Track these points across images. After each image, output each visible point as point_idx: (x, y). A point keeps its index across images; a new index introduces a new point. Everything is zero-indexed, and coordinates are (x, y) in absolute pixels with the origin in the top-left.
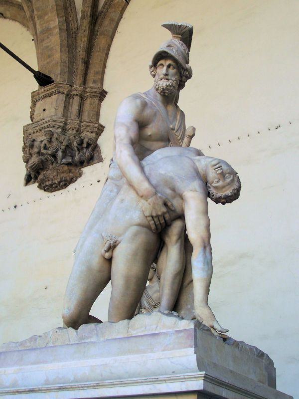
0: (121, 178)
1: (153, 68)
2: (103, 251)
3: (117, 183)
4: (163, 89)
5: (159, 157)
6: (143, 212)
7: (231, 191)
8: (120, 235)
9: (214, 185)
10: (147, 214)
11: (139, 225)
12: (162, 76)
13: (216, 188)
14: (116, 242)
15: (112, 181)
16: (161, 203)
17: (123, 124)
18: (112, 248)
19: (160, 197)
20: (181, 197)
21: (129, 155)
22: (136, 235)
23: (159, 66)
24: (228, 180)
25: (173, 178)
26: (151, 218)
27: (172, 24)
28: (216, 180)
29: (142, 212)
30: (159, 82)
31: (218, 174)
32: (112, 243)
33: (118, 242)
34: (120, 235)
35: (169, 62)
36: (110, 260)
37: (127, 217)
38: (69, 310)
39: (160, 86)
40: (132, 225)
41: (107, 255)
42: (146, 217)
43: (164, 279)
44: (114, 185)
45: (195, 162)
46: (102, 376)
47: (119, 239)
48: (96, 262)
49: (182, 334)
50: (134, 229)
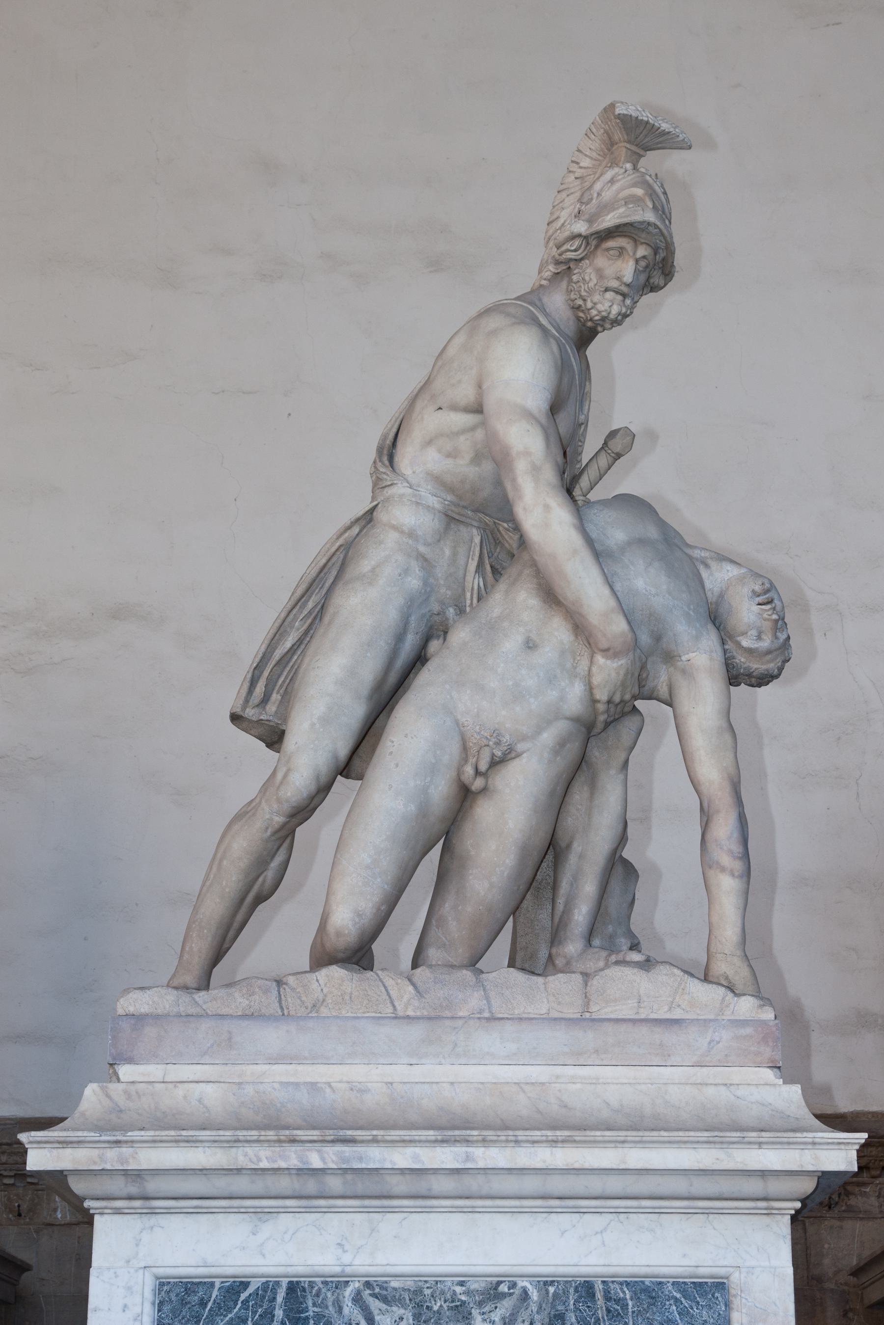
0: (439, 541)
1: (577, 243)
2: (469, 770)
3: (422, 549)
4: (604, 319)
8: (524, 738)
9: (745, 643)
10: (602, 695)
11: (576, 720)
12: (615, 284)
13: (750, 651)
14: (510, 753)
15: (410, 542)
17: (528, 415)
18: (496, 763)
20: (670, 658)
22: (561, 744)
24: (782, 637)
26: (606, 706)
27: (647, 122)
28: (754, 633)
29: (588, 687)
31: (765, 620)
32: (499, 753)
33: (513, 755)
37: (553, 695)
38: (359, 915)
39: (600, 307)
40: (557, 718)
41: (478, 783)
42: (594, 701)
43: (581, 857)
45: (697, 563)
47: (520, 747)
48: (441, 790)
49: (749, 1030)
50: (561, 727)
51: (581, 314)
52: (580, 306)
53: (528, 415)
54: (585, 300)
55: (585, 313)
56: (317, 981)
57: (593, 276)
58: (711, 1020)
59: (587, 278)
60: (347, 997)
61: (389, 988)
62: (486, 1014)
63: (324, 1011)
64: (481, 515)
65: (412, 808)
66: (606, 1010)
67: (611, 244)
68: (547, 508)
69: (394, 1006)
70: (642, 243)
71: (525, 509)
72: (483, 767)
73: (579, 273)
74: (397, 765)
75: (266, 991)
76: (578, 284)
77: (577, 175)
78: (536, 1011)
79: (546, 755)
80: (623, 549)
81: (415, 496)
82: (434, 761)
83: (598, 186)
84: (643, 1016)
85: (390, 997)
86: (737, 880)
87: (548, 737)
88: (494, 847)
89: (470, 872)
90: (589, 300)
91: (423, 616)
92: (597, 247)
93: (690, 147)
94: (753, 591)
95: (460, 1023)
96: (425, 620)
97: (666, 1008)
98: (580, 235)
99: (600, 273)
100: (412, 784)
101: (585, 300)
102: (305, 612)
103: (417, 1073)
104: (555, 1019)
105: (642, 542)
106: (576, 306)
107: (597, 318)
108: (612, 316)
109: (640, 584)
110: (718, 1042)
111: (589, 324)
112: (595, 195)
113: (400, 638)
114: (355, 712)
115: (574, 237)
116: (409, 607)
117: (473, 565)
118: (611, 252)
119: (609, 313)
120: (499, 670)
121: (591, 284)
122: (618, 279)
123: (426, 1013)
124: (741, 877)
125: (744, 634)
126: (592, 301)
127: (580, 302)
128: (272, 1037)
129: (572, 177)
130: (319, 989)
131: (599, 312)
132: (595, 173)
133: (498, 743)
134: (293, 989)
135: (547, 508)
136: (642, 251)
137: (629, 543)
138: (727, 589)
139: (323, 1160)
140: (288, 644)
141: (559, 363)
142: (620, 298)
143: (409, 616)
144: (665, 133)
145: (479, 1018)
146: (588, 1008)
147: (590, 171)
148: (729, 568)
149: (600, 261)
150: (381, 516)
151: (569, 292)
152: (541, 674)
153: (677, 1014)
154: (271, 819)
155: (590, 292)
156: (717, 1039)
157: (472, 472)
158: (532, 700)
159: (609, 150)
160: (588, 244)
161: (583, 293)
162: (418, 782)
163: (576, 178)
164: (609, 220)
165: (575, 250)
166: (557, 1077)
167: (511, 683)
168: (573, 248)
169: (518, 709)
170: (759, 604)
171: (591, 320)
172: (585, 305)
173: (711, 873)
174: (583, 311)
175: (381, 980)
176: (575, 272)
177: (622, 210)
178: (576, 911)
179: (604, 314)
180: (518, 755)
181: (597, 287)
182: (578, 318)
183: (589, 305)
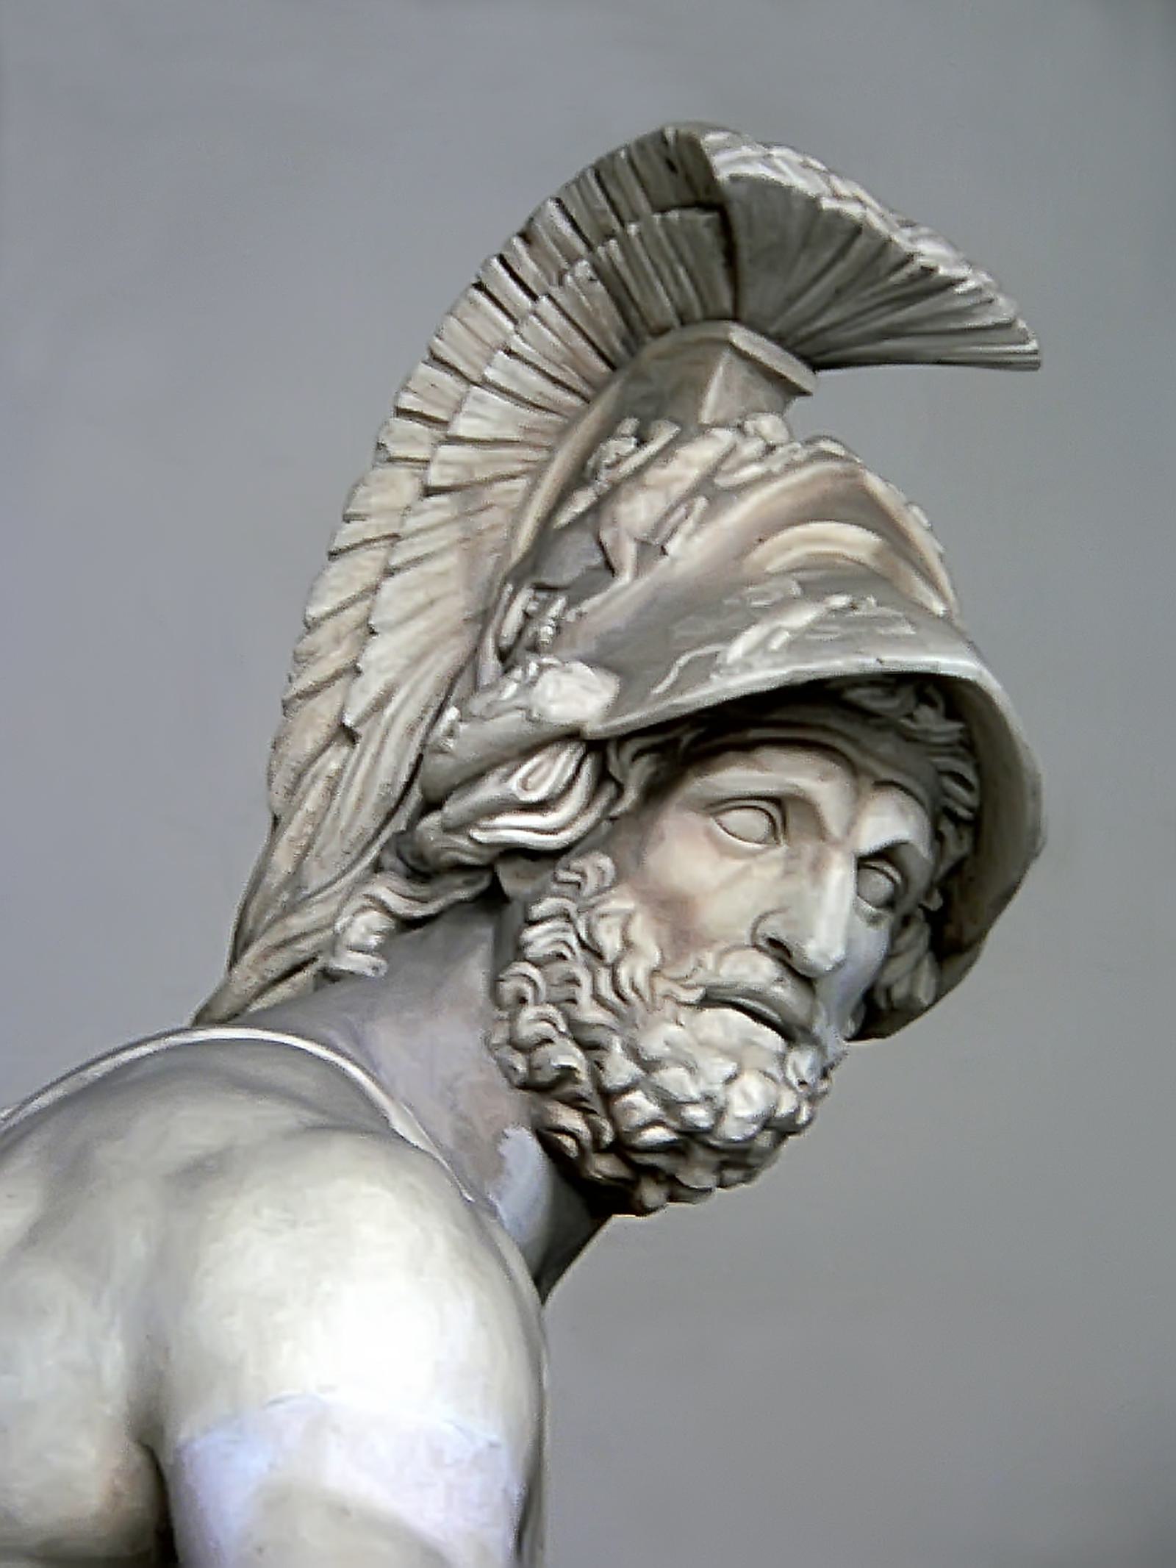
1: (553, 769)
23: (717, 807)
27: (857, 230)
35: (889, 822)
51: (571, 1119)
52: (567, 1074)
54: (589, 1047)
55: (586, 1112)
57: (642, 932)
59: (610, 942)
67: (735, 777)
70: (882, 784)
76: (559, 968)
90: (617, 1048)
92: (656, 792)
98: (571, 735)
99: (676, 916)
107: (657, 1135)
108: (732, 1131)
112: (629, 552)
118: (736, 818)
119: (719, 1114)
121: (634, 971)
122: (779, 950)
126: (634, 1053)
129: (405, 485)
131: (671, 1105)
132: (536, 472)
136: (889, 822)
142: (772, 1039)
144: (929, 284)
147: (510, 459)
160: (603, 777)
161: (590, 1013)
164: (751, 663)
165: (540, 807)
168: (534, 797)
172: (597, 1067)
174: (575, 1102)
176: (538, 910)
179: (699, 1116)
181: (662, 986)
182: (547, 1137)
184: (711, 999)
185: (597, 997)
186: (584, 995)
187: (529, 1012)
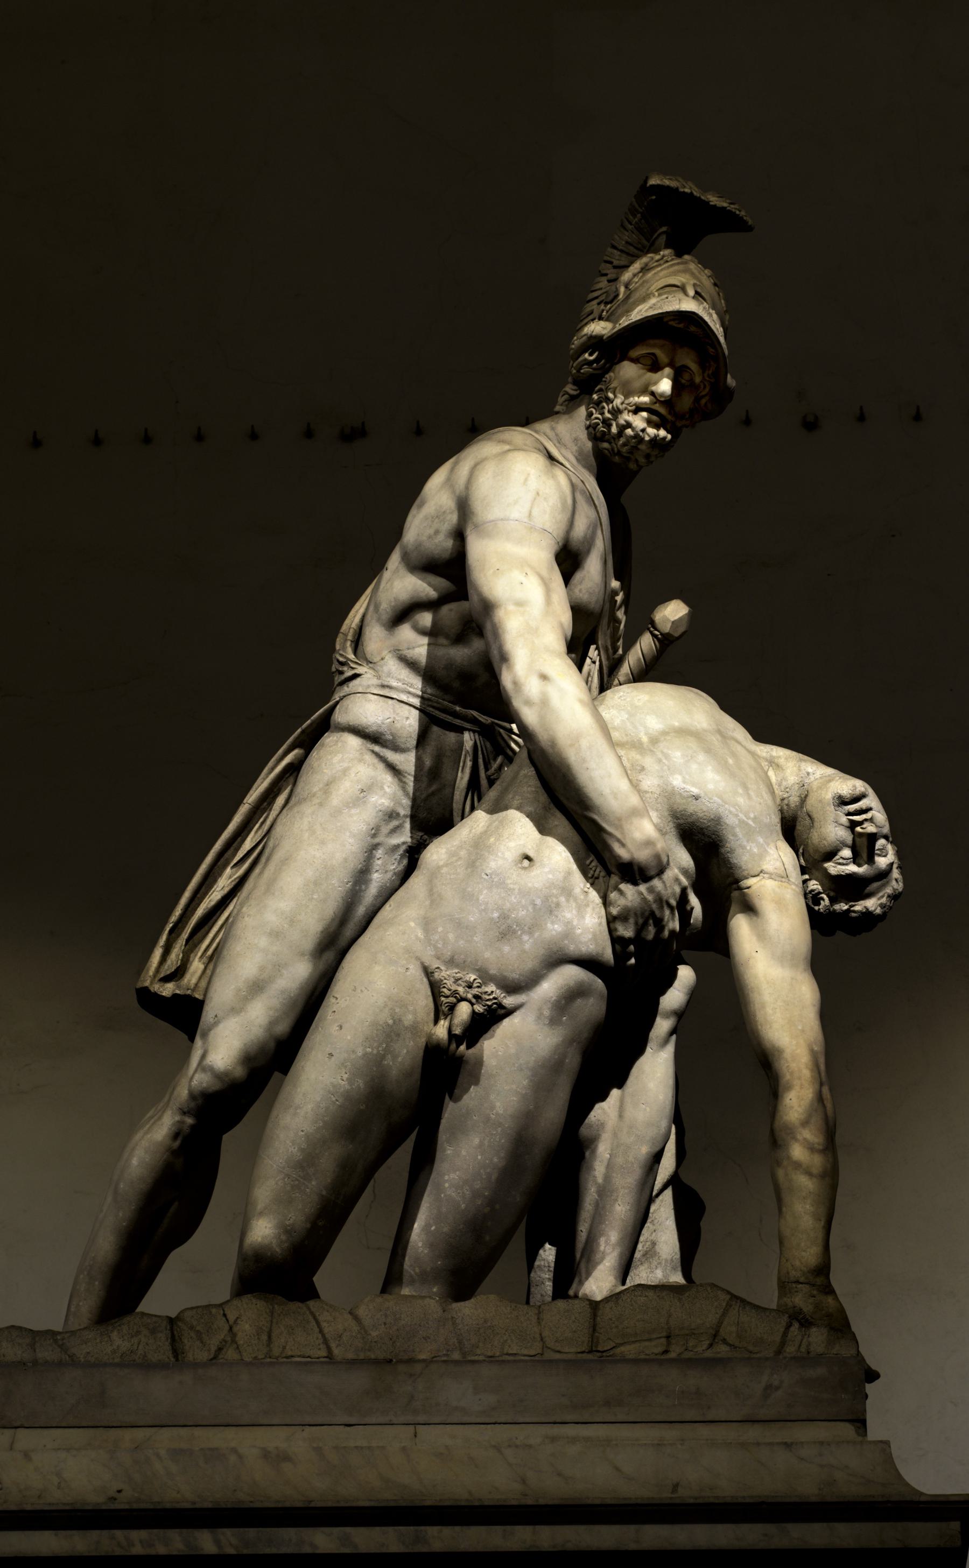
5: (654, 724)
6: (611, 920)
7: (884, 900)
8: (513, 988)
9: (833, 868)
11: (588, 963)
12: (645, 399)
15: (377, 748)
16: (673, 902)
17: (523, 564)
19: (677, 880)
21: (581, 701)
25: (718, 820)
28: (847, 853)
30: (627, 417)
31: (861, 834)
34: (513, 988)
36: (444, 1070)
37: (554, 928)
44: (381, 766)
46: (524, 1481)
47: (509, 1001)
50: (571, 974)
53: (523, 564)
55: (610, 443)
56: (225, 1315)
58: (767, 1359)
60: (264, 1337)
61: (324, 1325)
62: (456, 1356)
63: (230, 1354)
64: (475, 713)
65: (360, 1083)
66: (622, 1349)
68: (544, 677)
69: (329, 1349)
71: (515, 683)
72: (457, 1031)
73: (601, 390)
74: (341, 1027)
75: (153, 1331)
77: (609, 277)
78: (526, 1352)
79: (547, 1013)
80: (654, 741)
81: (383, 686)
82: (390, 1022)
83: (626, 276)
84: (672, 1355)
85: (323, 1336)
86: (815, 1180)
87: (551, 986)
88: (476, 1141)
89: (446, 1177)
91: (397, 847)
93: (749, 229)
94: (840, 797)
95: (418, 1368)
96: (397, 856)
97: (705, 1347)
100: (360, 1052)
101: (610, 426)
102: (240, 854)
103: (358, 1437)
104: (550, 1361)
105: (683, 732)
106: (598, 435)
109: (677, 781)
110: (777, 1388)
111: (617, 459)
112: (622, 289)
113: (362, 875)
114: (299, 972)
115: (595, 343)
116: (374, 836)
117: (463, 779)
120: (481, 897)
123: (373, 1357)
124: (823, 1176)
125: (831, 855)
126: (617, 425)
127: (601, 428)
128: (161, 1390)
130: (227, 1327)
133: (477, 997)
134: (192, 1328)
135: (544, 677)
137: (665, 733)
138: (806, 796)
139: (217, 1542)
140: (215, 895)
141: (570, 501)
143: (375, 847)
145: (444, 1361)
146: (596, 1346)
148: (810, 770)
149: (628, 370)
150: (339, 717)
151: (590, 415)
152: (538, 902)
153: (722, 1350)
154: (181, 1122)
155: (616, 412)
156: (776, 1383)
157: (460, 654)
158: (525, 938)
159: (648, 240)
161: (608, 415)
162: (369, 1050)
163: (609, 281)
166: (553, 1439)
167: (496, 915)
168: (591, 358)
169: (506, 949)
170: (849, 814)
171: (619, 453)
173: (780, 1173)
175: (312, 1314)
177: (653, 301)
178: (602, 1241)
180: (509, 1012)
181: (624, 406)
183: (614, 429)
184: (637, 409)
185: (609, 411)
186: (606, 411)
187: (594, 416)
